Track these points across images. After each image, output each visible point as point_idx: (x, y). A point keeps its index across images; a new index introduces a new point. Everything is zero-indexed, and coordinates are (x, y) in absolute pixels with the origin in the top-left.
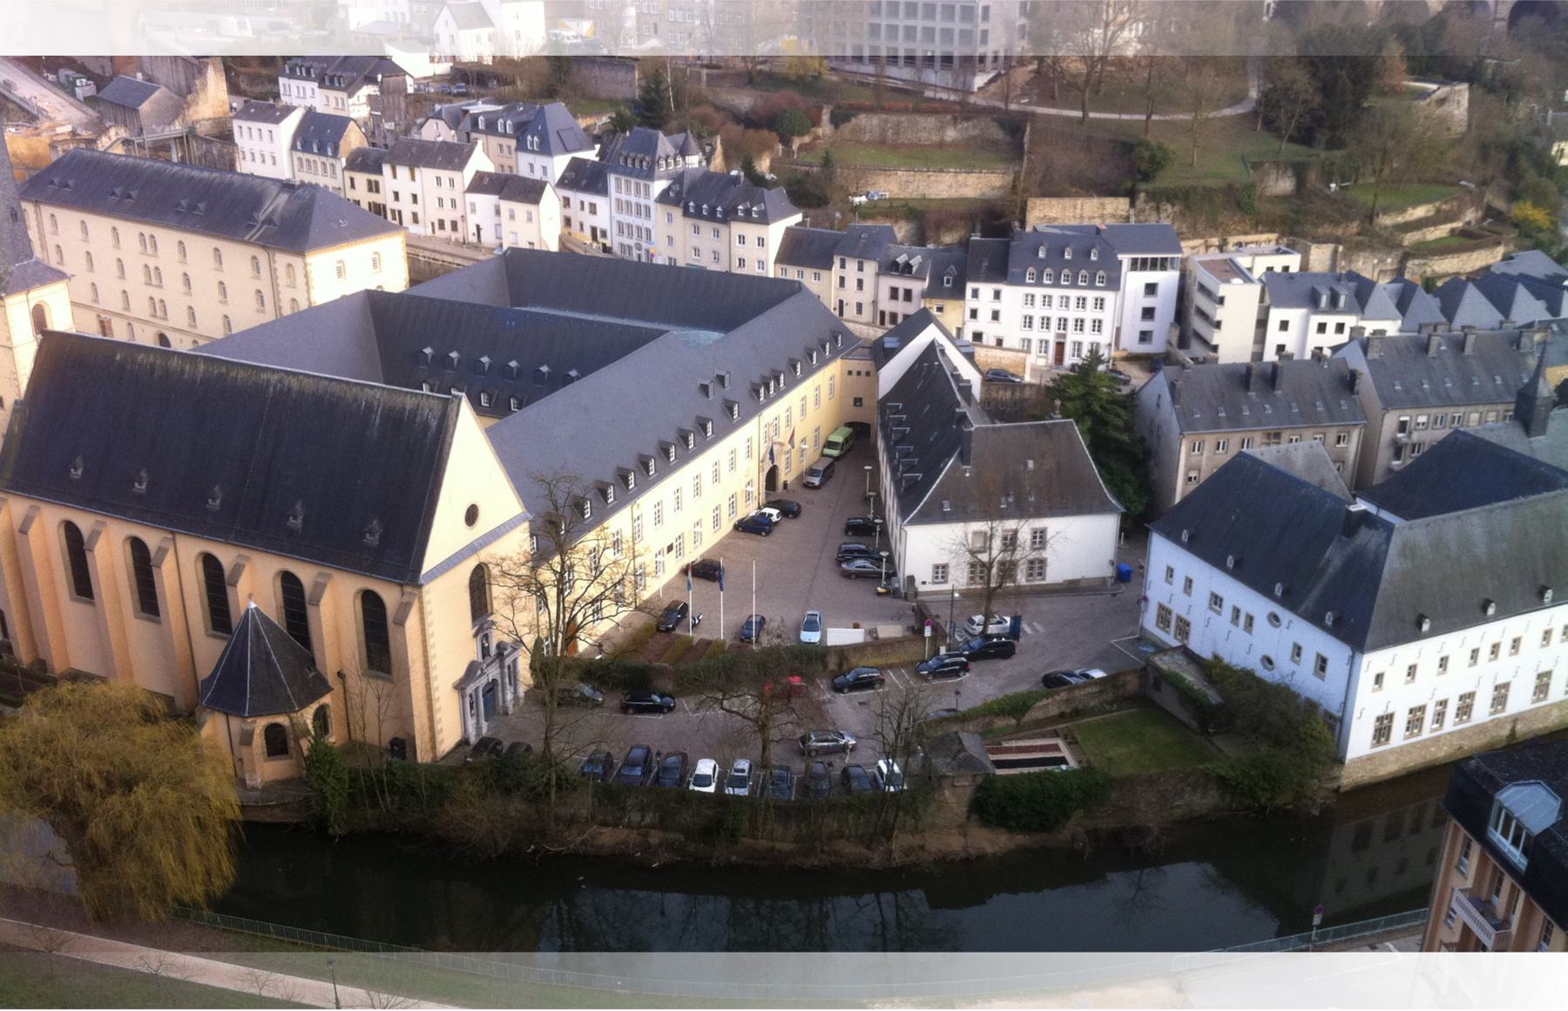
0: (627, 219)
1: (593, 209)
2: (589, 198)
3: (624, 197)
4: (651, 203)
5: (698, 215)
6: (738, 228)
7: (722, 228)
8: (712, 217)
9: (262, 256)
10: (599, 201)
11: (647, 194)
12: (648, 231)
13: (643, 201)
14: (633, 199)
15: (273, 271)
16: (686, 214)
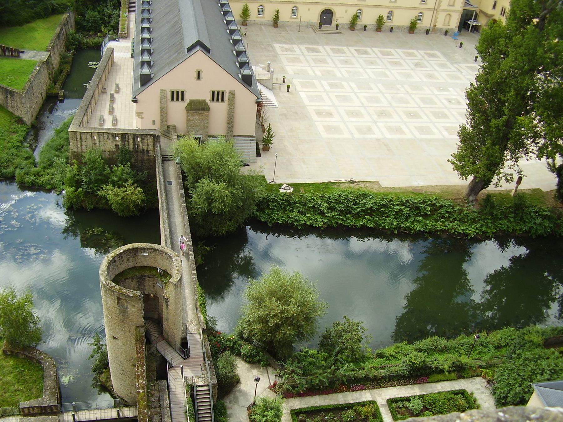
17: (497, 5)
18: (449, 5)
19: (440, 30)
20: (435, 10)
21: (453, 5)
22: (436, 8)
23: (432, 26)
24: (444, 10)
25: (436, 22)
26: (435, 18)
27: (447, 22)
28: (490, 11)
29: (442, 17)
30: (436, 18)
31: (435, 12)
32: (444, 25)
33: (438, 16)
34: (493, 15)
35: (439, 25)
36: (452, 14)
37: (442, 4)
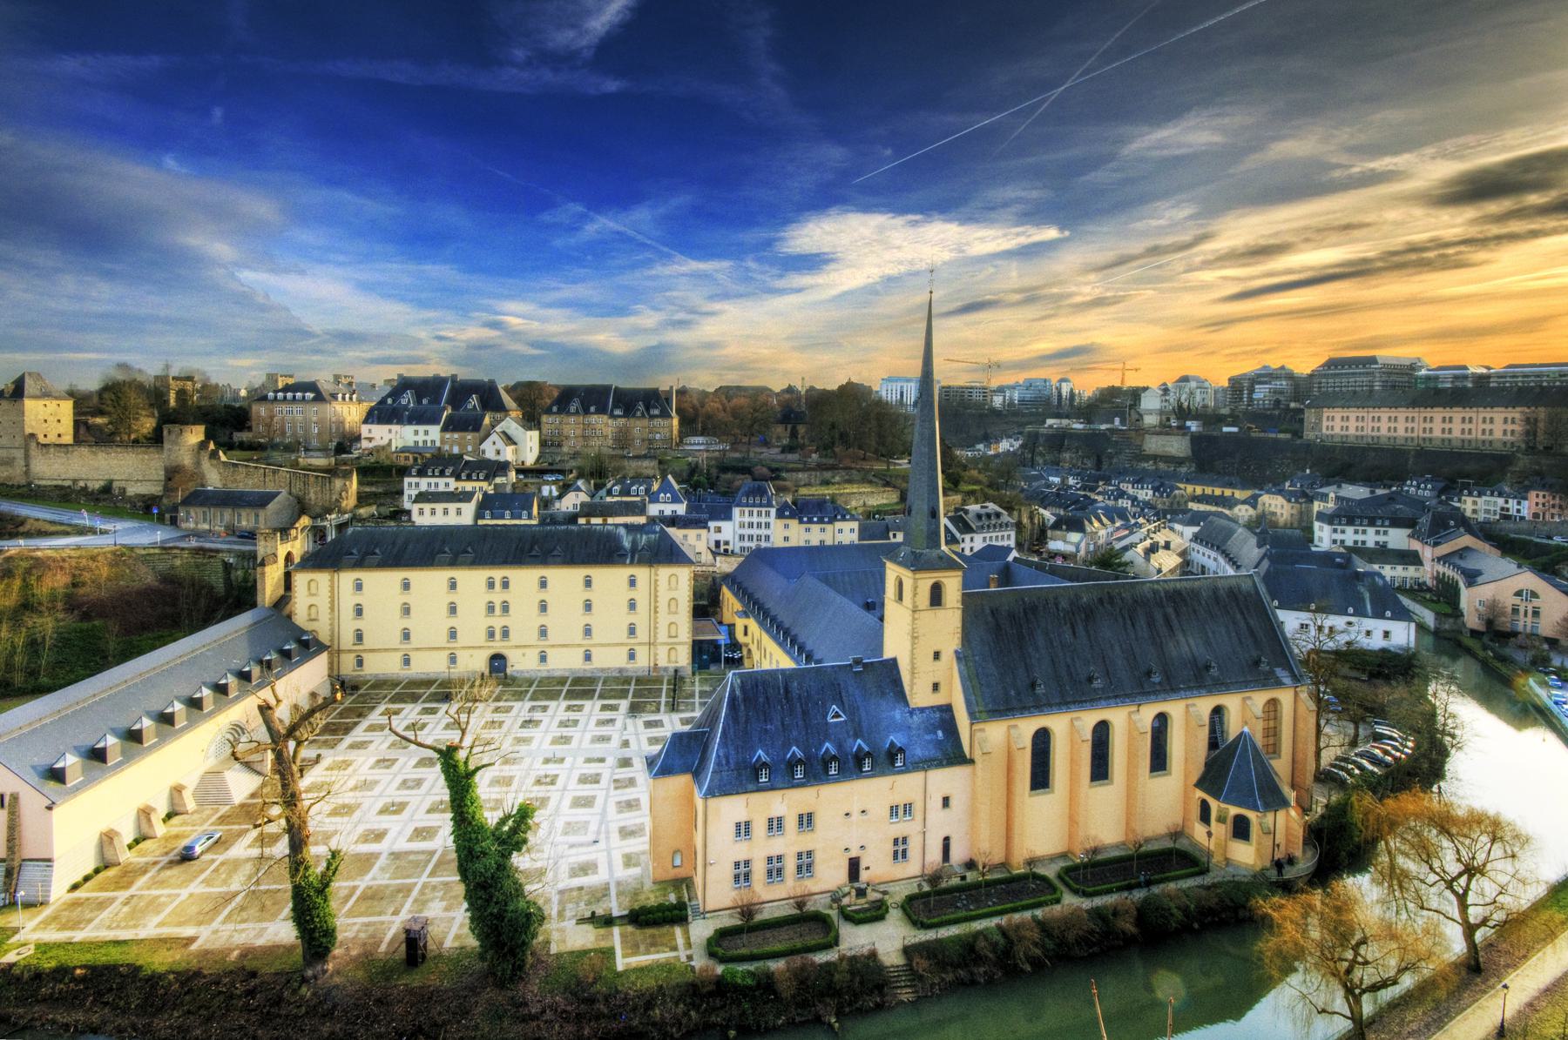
0: (747, 532)
1: (719, 530)
2: (712, 524)
3: (747, 519)
4: (772, 519)
5: (810, 521)
6: (838, 525)
7: (829, 527)
8: (821, 521)
9: (642, 573)
10: (723, 524)
11: (768, 514)
12: (767, 538)
13: (763, 520)
14: (755, 519)
16: (801, 522)
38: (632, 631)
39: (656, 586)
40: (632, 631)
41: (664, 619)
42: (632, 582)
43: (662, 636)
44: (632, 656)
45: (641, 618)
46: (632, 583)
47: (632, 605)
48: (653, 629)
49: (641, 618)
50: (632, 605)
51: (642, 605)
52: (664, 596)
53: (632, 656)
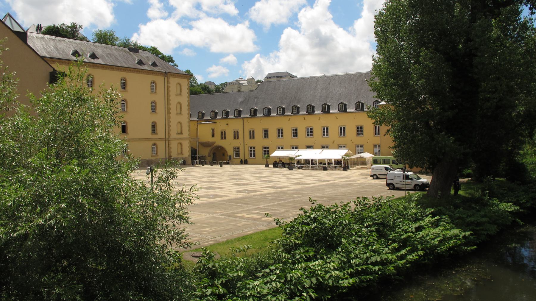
9: (160, 80)
15: (167, 90)
17: (215, 133)
18: (178, 134)
19: (177, 159)
20: (167, 140)
21: (181, 133)
22: (167, 137)
23: (167, 157)
24: (175, 139)
25: (170, 152)
26: (168, 148)
27: (180, 152)
28: (210, 139)
29: (174, 145)
30: (170, 148)
31: (167, 142)
32: (178, 154)
33: (171, 146)
34: (215, 143)
35: (174, 155)
36: (182, 142)
37: (171, 132)
38: (154, 128)
39: (169, 91)
40: (154, 128)
41: (174, 119)
42: (153, 88)
43: (174, 135)
44: (154, 149)
45: (160, 118)
46: (153, 88)
47: (154, 108)
48: (168, 126)
49: (160, 118)
50: (154, 108)
51: (160, 108)
52: (174, 100)
53: (154, 149)
